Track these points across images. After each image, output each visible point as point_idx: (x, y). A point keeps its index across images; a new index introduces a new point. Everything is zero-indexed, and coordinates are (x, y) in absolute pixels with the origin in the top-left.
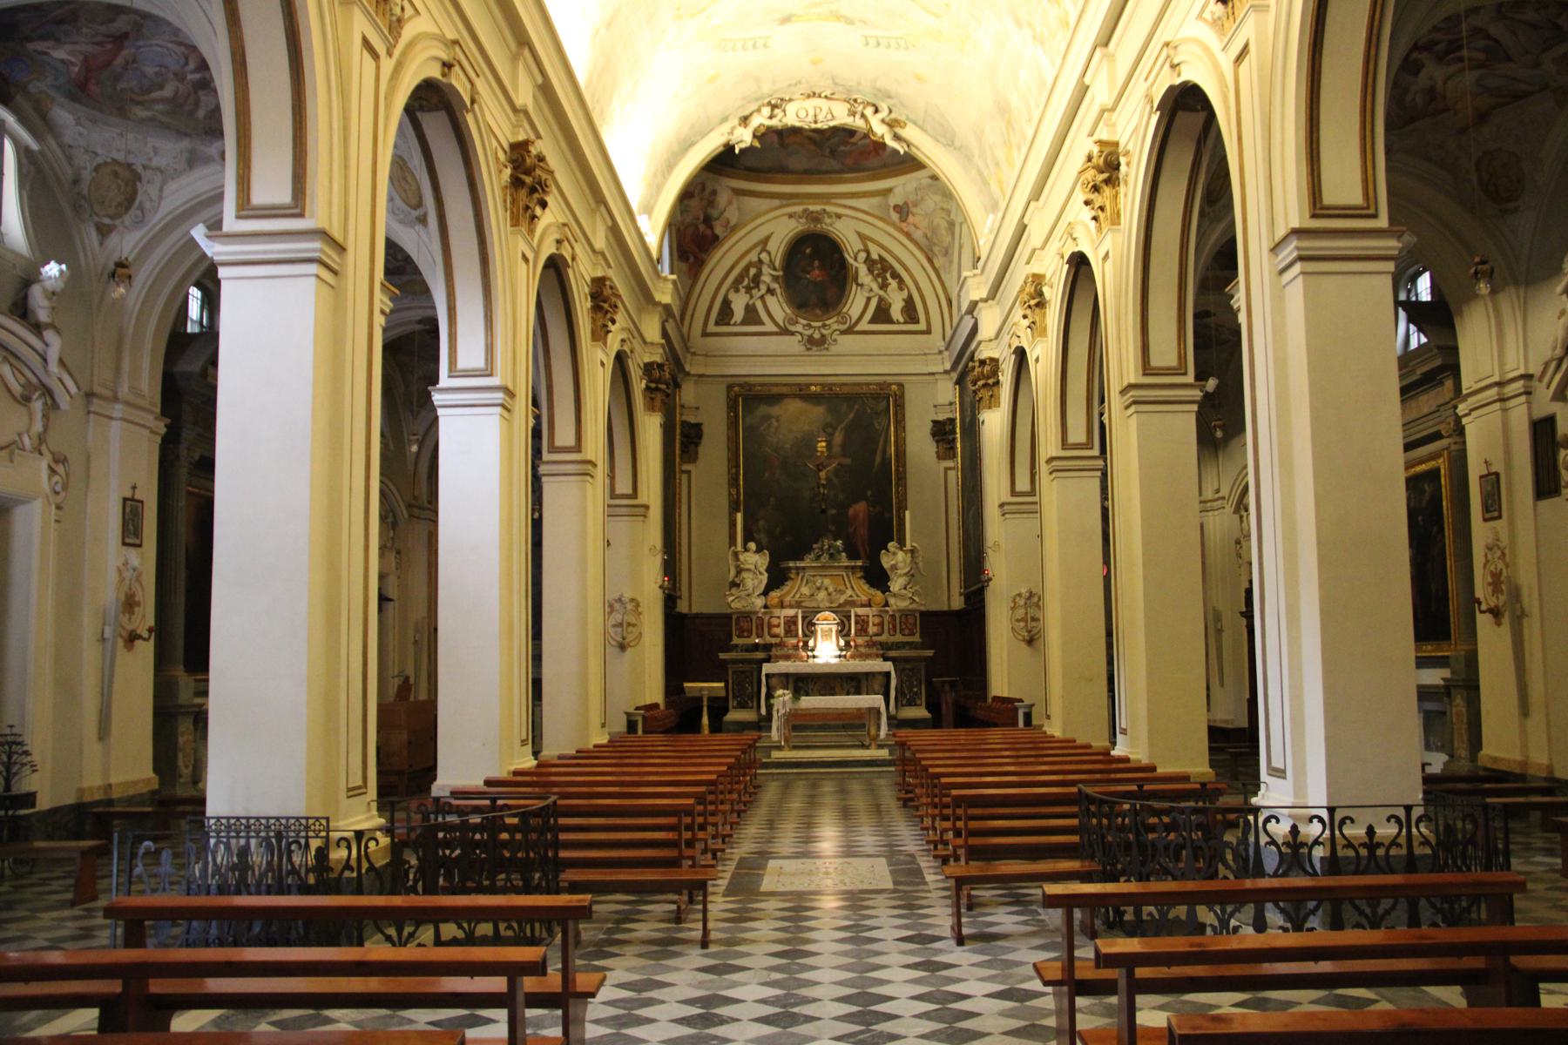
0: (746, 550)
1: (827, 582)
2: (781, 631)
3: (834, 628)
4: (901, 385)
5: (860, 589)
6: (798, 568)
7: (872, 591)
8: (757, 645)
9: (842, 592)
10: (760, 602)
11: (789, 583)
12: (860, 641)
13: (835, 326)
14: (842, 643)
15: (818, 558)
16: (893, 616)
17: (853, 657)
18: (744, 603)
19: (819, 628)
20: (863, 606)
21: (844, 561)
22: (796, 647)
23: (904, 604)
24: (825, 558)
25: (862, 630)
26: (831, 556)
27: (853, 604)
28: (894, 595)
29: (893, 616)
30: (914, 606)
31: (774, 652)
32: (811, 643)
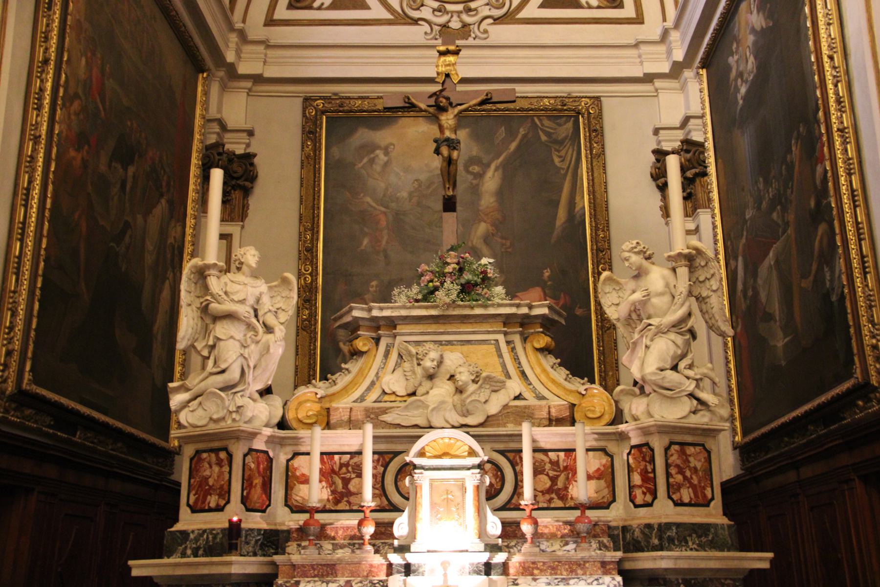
0: (229, 264)
1: (453, 359)
2: (316, 492)
3: (472, 479)
4: (597, 100)
5: (548, 381)
6: (376, 324)
7: (579, 385)
8: (234, 529)
9: (496, 386)
10: (261, 414)
11: (353, 366)
12: (548, 520)
13: (486, 11)
14: (494, 526)
15: (429, 295)
16: (644, 451)
17: (528, 570)
18: (213, 409)
19: (423, 479)
20: (553, 421)
21: (499, 301)
22: (355, 540)
23: (675, 413)
24: (448, 292)
25: (554, 493)
26: (466, 289)
27: (525, 415)
28: (640, 387)
29: (644, 451)
30: (702, 419)
31: (296, 554)
32: (400, 527)
